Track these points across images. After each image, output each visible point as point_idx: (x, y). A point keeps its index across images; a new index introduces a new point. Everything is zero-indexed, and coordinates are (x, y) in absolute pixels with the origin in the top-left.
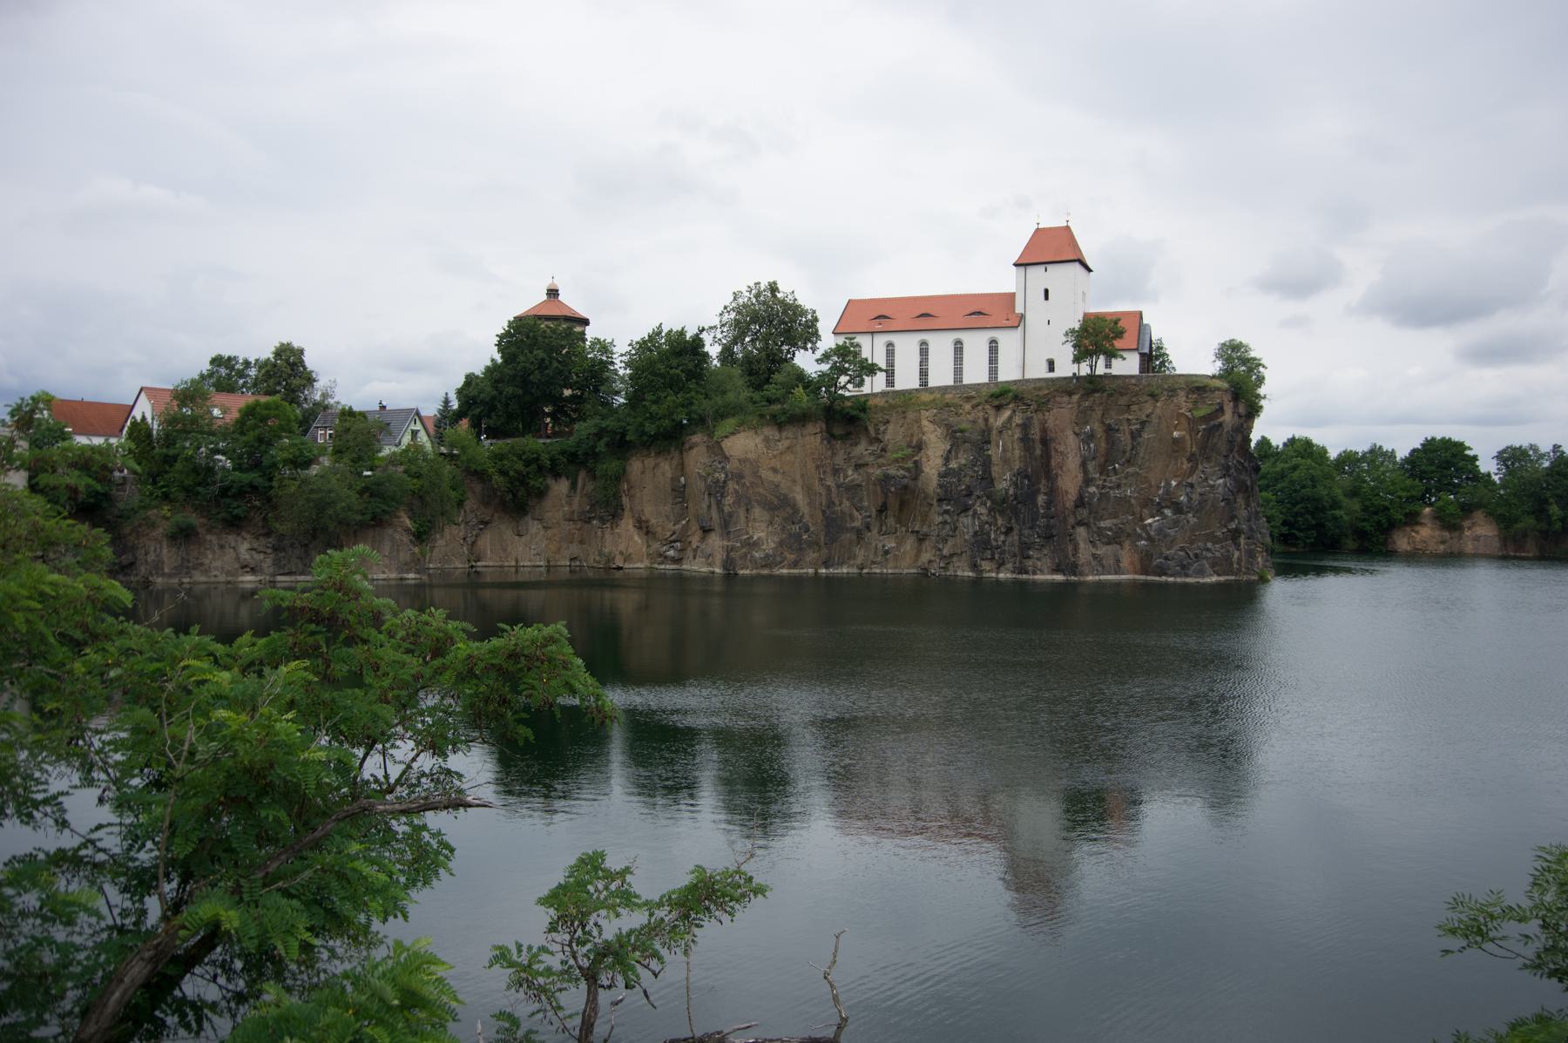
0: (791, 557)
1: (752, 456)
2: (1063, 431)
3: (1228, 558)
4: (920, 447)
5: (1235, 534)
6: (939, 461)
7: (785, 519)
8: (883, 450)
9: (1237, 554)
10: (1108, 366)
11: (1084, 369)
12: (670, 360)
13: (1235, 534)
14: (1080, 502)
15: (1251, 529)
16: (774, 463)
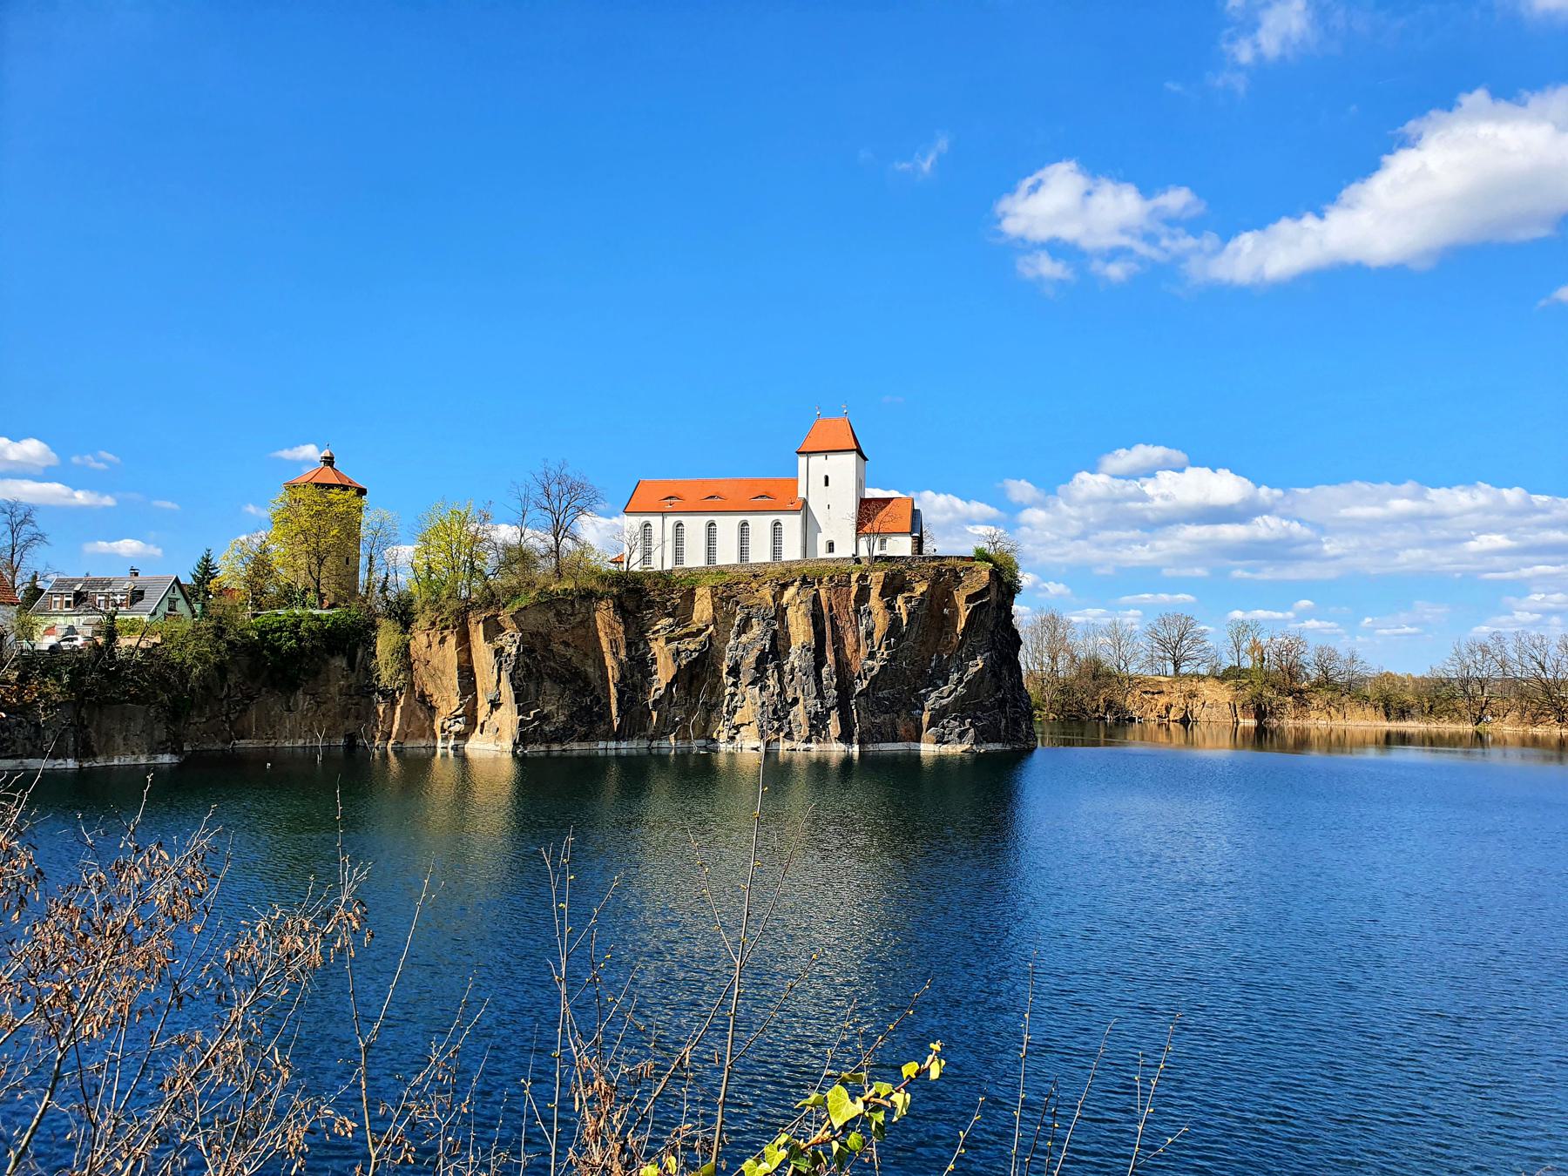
3: (995, 724)
7: (576, 692)
13: (1002, 703)
16: (568, 637)
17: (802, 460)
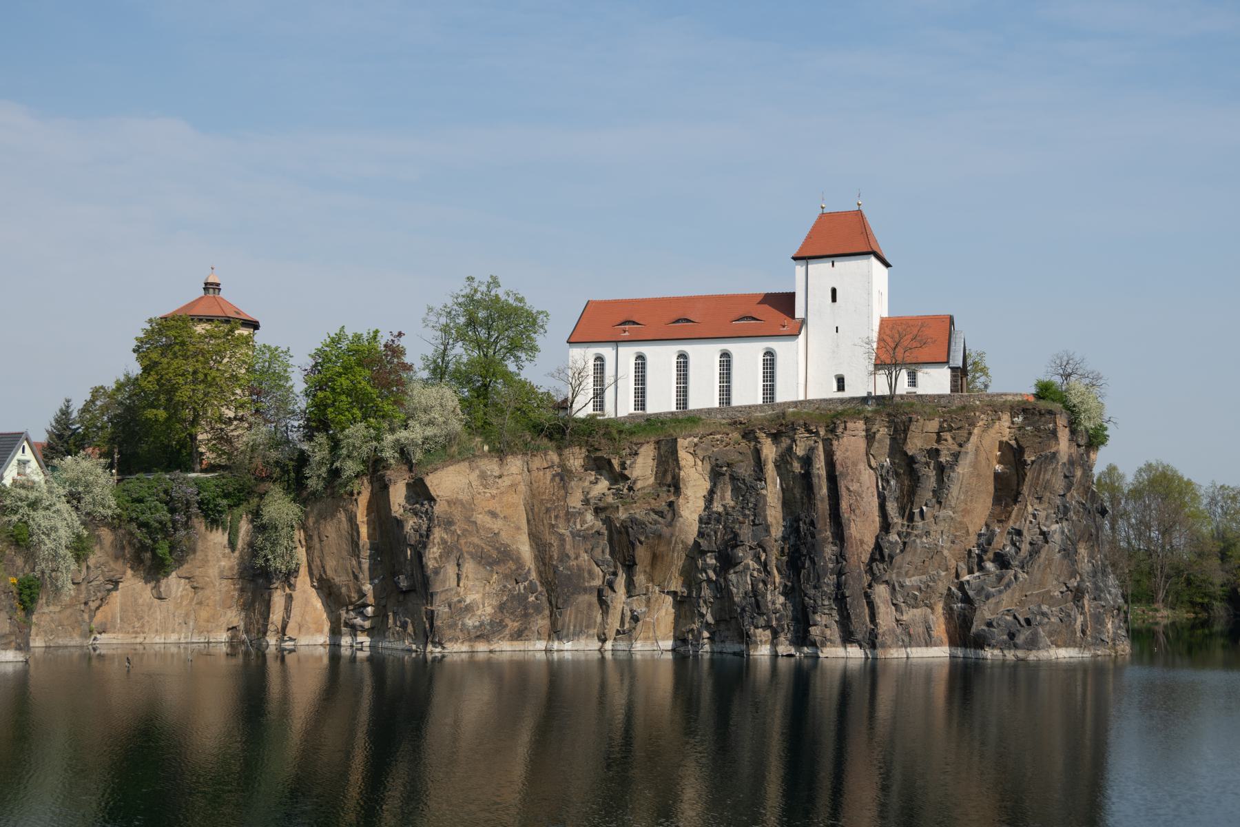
0: (513, 625)
1: (464, 497)
2: (855, 464)
4: (676, 486)
5: (1078, 594)
6: (702, 504)
7: (506, 577)
8: (630, 489)
9: (1080, 619)
10: (913, 383)
11: (882, 389)
12: (361, 377)
14: (879, 553)
15: (1097, 588)
16: (494, 505)
17: (800, 269)
